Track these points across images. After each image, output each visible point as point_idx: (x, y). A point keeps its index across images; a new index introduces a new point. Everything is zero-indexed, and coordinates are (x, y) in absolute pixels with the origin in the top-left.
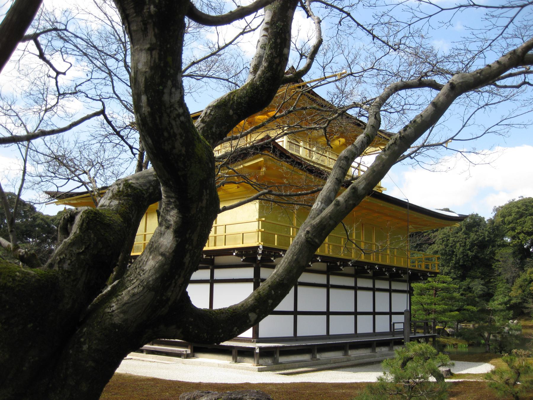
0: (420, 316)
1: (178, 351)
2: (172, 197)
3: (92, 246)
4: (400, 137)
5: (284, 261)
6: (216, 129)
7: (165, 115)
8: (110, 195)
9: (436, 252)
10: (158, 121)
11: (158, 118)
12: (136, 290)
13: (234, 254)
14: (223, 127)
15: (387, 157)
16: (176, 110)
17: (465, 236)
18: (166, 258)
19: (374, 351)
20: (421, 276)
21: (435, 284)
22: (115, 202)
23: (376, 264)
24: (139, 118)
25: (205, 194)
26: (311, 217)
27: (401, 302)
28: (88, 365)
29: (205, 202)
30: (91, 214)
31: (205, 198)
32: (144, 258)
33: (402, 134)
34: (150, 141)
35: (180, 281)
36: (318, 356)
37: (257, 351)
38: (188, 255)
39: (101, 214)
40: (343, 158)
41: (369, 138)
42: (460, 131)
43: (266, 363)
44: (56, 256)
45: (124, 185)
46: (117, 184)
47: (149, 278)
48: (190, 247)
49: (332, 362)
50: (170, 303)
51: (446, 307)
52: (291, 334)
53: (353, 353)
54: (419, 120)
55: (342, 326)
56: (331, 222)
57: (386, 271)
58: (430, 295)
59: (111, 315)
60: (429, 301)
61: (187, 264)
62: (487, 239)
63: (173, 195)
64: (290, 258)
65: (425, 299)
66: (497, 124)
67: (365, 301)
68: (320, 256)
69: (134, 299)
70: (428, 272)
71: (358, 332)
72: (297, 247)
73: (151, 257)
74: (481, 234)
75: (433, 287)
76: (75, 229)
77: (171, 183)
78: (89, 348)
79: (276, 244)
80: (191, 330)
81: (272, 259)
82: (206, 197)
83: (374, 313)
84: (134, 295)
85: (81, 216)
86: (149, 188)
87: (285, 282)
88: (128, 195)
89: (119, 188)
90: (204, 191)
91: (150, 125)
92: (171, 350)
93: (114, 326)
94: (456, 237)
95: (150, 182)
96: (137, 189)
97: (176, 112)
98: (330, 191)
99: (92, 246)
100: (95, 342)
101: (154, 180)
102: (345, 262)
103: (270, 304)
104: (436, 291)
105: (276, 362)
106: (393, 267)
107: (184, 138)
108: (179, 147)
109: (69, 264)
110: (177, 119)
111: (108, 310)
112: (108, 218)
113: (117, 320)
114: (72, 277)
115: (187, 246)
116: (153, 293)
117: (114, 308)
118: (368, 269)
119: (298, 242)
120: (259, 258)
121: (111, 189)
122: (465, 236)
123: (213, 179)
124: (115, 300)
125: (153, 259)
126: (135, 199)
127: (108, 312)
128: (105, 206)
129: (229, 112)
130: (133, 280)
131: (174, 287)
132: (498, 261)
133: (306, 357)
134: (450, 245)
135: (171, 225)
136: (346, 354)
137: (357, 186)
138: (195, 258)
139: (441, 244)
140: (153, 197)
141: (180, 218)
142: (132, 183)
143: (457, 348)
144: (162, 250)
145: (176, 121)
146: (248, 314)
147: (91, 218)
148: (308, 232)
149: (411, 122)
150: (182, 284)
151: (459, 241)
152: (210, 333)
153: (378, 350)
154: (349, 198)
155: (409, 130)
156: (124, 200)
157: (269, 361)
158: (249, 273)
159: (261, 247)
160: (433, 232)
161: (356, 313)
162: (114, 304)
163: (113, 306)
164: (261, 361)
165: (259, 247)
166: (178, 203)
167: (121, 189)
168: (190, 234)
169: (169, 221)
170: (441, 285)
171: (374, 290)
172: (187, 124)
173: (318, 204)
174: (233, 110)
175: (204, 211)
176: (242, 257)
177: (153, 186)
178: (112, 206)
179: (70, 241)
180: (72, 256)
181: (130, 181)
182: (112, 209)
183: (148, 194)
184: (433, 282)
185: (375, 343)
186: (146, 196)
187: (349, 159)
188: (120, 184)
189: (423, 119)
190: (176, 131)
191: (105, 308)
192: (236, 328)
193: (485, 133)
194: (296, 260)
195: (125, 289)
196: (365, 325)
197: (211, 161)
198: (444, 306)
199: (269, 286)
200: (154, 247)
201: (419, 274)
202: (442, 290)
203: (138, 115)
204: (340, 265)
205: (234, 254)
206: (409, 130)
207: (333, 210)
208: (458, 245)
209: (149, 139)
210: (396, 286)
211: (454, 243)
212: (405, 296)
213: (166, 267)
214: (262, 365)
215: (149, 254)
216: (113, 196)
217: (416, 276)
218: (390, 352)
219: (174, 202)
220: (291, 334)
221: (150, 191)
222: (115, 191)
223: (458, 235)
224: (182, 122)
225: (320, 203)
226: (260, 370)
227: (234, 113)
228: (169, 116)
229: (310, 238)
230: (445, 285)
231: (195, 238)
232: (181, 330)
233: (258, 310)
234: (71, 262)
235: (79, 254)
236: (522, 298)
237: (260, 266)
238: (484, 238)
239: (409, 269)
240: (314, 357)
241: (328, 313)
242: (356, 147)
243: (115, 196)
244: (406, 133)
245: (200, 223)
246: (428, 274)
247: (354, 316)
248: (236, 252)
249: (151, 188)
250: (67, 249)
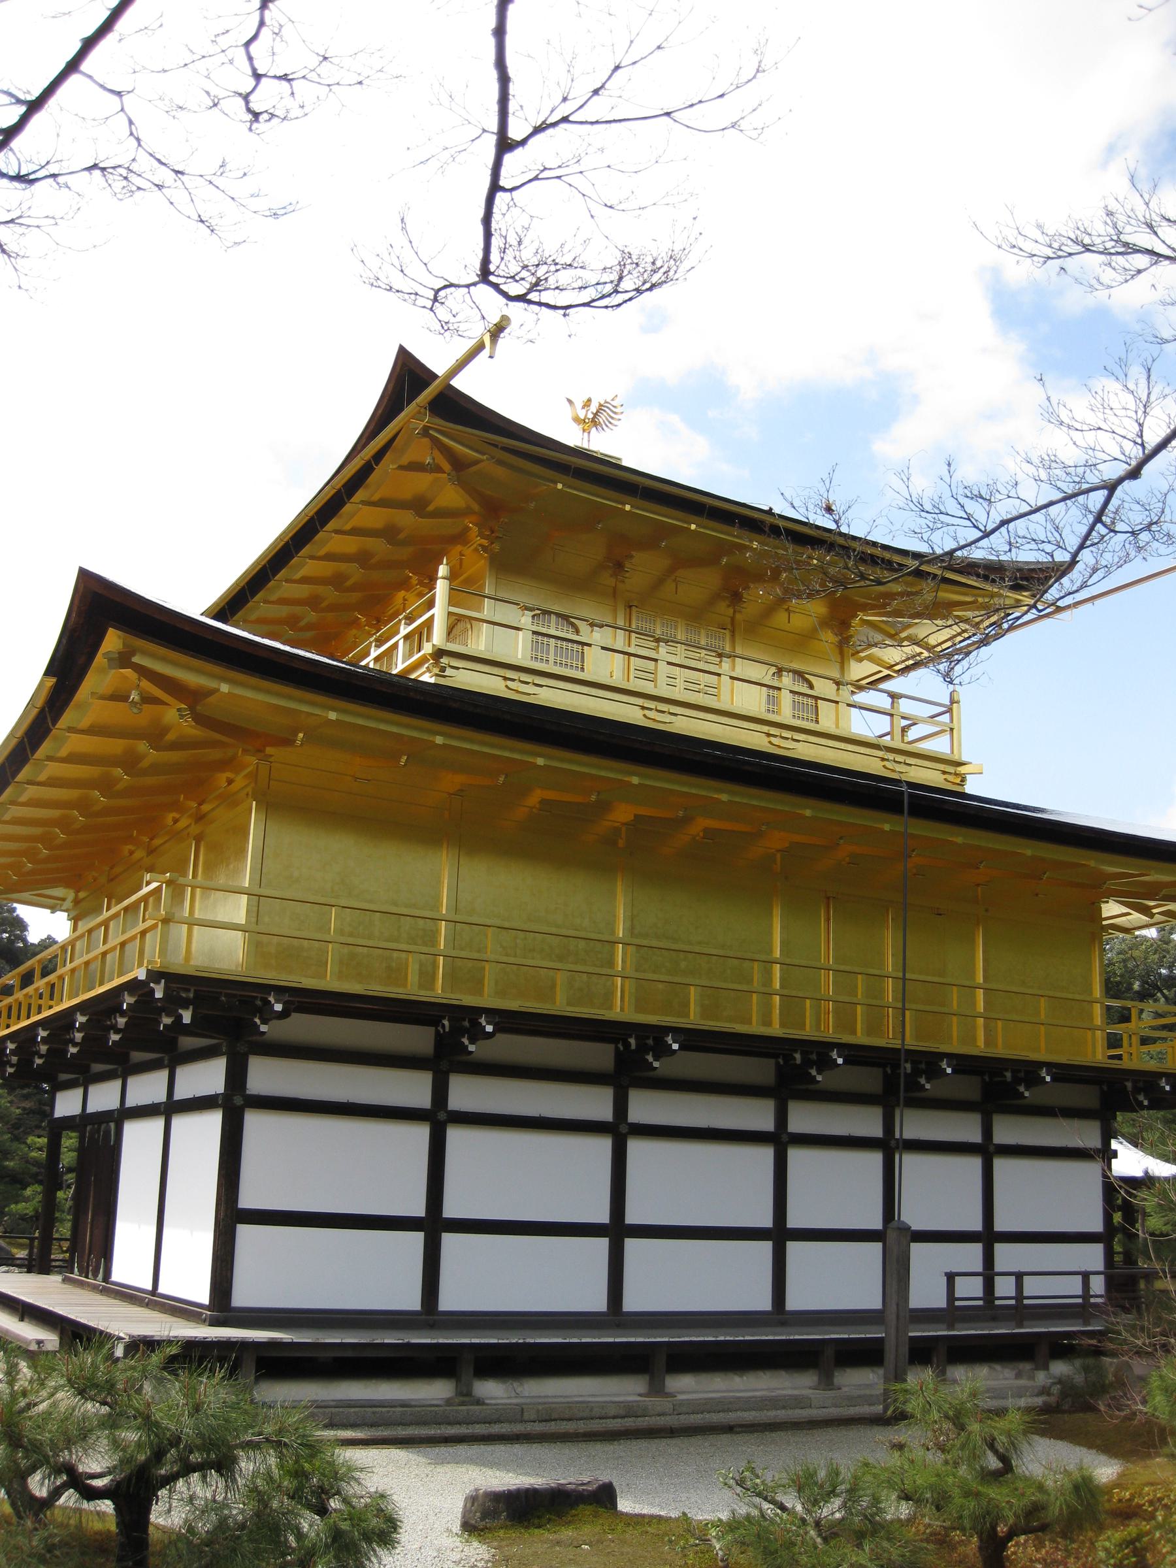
19: (827, 1382)
20: (1137, 1090)
52: (412, 1301)
53: (686, 1387)
68: (491, 1013)
81: (257, 1020)
133: (433, 1392)
136: (657, 1389)
201: (1129, 1085)
204: (643, 1048)
220: (412, 1301)
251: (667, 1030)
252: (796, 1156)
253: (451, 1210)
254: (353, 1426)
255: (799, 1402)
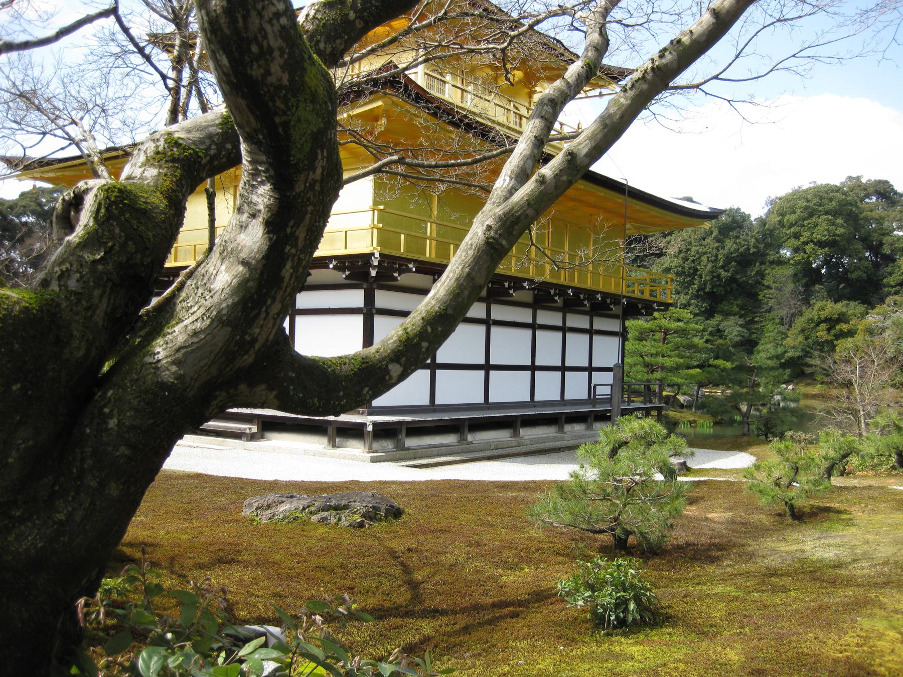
0: (638, 375)
1: (236, 428)
2: (261, 163)
3: (117, 248)
4: (653, 68)
5: (448, 277)
6: (326, 43)
7: (253, 14)
8: (142, 158)
9: (668, 270)
10: (241, 23)
11: (240, 20)
12: (198, 325)
13: (331, 266)
14: (338, 41)
15: (629, 102)
16: (273, 4)
17: (716, 245)
18: (250, 269)
19: (561, 429)
20: (643, 308)
21: (665, 323)
22: (152, 172)
23: (569, 287)
24: (205, 18)
25: (320, 157)
26: (494, 202)
27: (607, 351)
28: (118, 454)
29: (319, 171)
30: (113, 192)
31: (320, 164)
32: (211, 269)
33: (657, 63)
34: (225, 61)
35: (276, 308)
36: (470, 437)
37: (370, 428)
38: (289, 265)
39: (130, 192)
40: (546, 101)
41: (591, 68)
42: (730, 65)
43: (384, 448)
44: (53, 266)
45: (166, 140)
46: (153, 140)
47: (220, 304)
48: (293, 251)
49: (492, 447)
50: (257, 346)
51: (682, 361)
52: (426, 401)
53: (528, 434)
54: (686, 40)
55: (509, 389)
56: (530, 212)
57: (585, 299)
58: (655, 340)
59: (155, 368)
60: (653, 351)
61: (286, 280)
62: (752, 250)
63: (264, 158)
64: (458, 271)
65: (648, 346)
66: (794, 56)
67: (549, 348)
69: (195, 340)
70: (654, 302)
71: (537, 398)
72: (471, 253)
73: (223, 267)
74: (743, 243)
75: (661, 328)
76: (85, 218)
77: (261, 137)
78: (120, 424)
79: (402, 251)
80: (291, 393)
81: (396, 275)
82: (321, 163)
83: (563, 369)
84: (195, 333)
85: (96, 196)
86: (208, 149)
87: (450, 312)
88: (174, 160)
89: (157, 147)
90: (319, 151)
91: (227, 31)
92: (225, 427)
93: (162, 386)
94: (701, 245)
95: (210, 136)
96: (189, 149)
97: (273, 9)
98: (526, 159)
99: (117, 248)
100: (128, 414)
101: (217, 134)
102: (517, 282)
103: (424, 350)
104: (666, 334)
105: (400, 447)
106: (598, 292)
107: (286, 56)
108: (278, 73)
109: (78, 281)
110: (275, 22)
111: (149, 359)
112: (143, 200)
113: (169, 374)
114: (84, 303)
115: (288, 248)
116: (229, 329)
117: (160, 356)
118: (555, 294)
119: (472, 245)
120: (373, 273)
121: (144, 148)
122: (716, 245)
123: (333, 131)
124: (162, 342)
125: (227, 270)
126: (194, 166)
127: (151, 363)
128: (133, 178)
129: (348, 14)
130: (191, 306)
131: (265, 319)
132: (769, 287)
133: (450, 439)
134: (692, 258)
135: (260, 211)
136: (516, 434)
137: (575, 151)
138: (301, 270)
139: (677, 257)
140: (216, 163)
141: (275, 198)
142: (179, 138)
143: (695, 427)
144: (243, 255)
145: (272, 25)
146: (387, 366)
147: (113, 199)
148: (489, 228)
149: (672, 42)
150: (278, 314)
151: (706, 253)
152: (319, 398)
153: (568, 428)
154: (561, 171)
155: (668, 57)
156: (168, 168)
157: (389, 445)
158: (356, 298)
159: (377, 255)
160: (665, 236)
161: (533, 368)
162: (158, 349)
163: (158, 353)
164: (376, 445)
165: (373, 254)
166: (272, 172)
167: (161, 149)
168: (292, 227)
169: (255, 204)
170: (674, 325)
171: (564, 330)
172: (292, 32)
173: (504, 180)
174: (355, 12)
175: (317, 187)
176: (344, 272)
177: (216, 144)
178: (146, 179)
179: (77, 240)
180: (81, 266)
181: (176, 135)
182: (148, 183)
183: (208, 158)
184: (661, 320)
185: (563, 418)
186: (204, 161)
187: (556, 104)
188: (158, 140)
189: (694, 37)
190: (272, 42)
191: (145, 356)
192: (367, 389)
193: (771, 70)
194: (469, 274)
195: (177, 323)
196: (548, 388)
197: (331, 100)
198: (677, 359)
199: (423, 318)
200: (229, 249)
201: (640, 306)
202: (676, 332)
203: (203, 12)
204: (510, 288)
205: (331, 266)
206: (668, 57)
207: (532, 191)
208: (704, 258)
209: (224, 57)
210: (600, 324)
211: (697, 256)
212: (615, 341)
213: (251, 284)
214: (377, 452)
215: (219, 262)
216: (148, 160)
217: (635, 308)
218: (588, 433)
219: (264, 172)
220: (426, 401)
221: (212, 152)
222: (150, 152)
223: (705, 243)
224: (283, 28)
225: (508, 179)
226: (374, 460)
227: (356, 17)
228: (260, 15)
229: (492, 237)
230: (680, 324)
231: (301, 233)
232: (274, 393)
233: (404, 359)
234: (81, 277)
235: (95, 262)
236: (802, 350)
237: (375, 286)
238: (748, 249)
239: (624, 297)
240: (463, 439)
241: (487, 367)
242: (568, 83)
243: (152, 161)
244: (664, 61)
245: (310, 208)
246: (655, 305)
247: (529, 372)
248: (334, 263)
249: (214, 147)
250: (73, 254)
251: (524, 280)
252: (539, 333)
253: (586, 365)
254: (450, 454)
255: (543, 440)
